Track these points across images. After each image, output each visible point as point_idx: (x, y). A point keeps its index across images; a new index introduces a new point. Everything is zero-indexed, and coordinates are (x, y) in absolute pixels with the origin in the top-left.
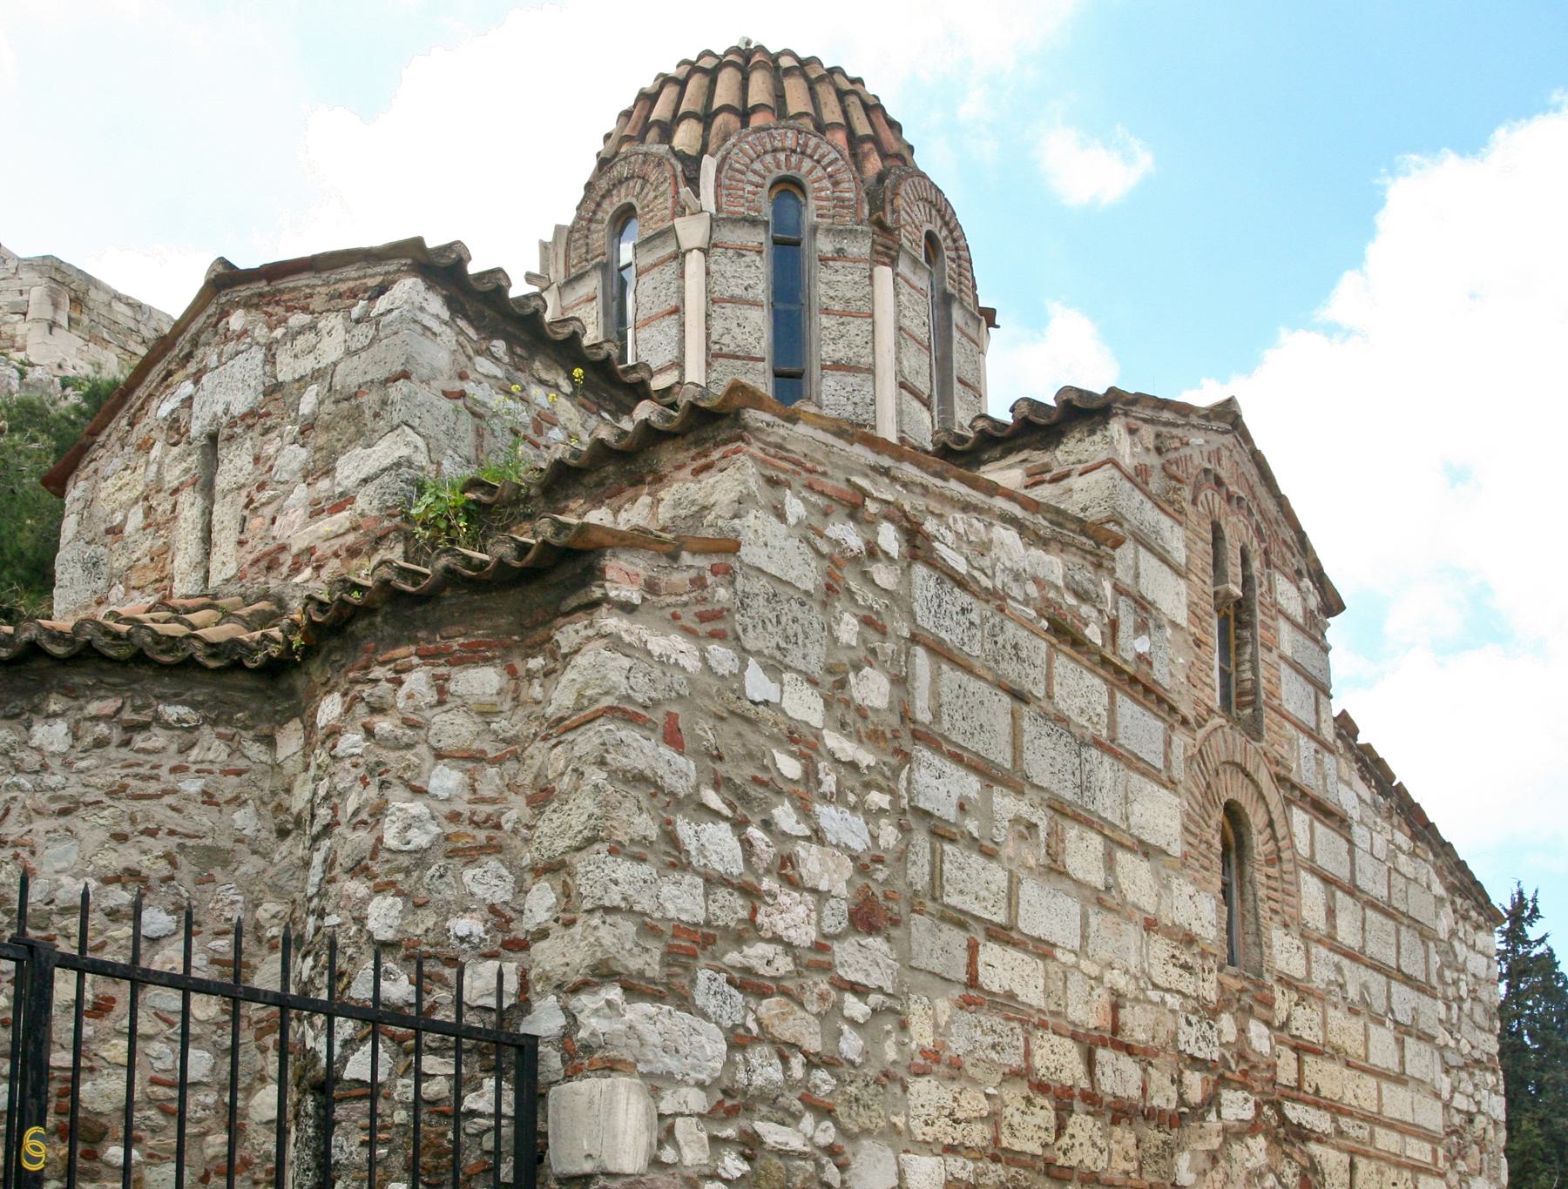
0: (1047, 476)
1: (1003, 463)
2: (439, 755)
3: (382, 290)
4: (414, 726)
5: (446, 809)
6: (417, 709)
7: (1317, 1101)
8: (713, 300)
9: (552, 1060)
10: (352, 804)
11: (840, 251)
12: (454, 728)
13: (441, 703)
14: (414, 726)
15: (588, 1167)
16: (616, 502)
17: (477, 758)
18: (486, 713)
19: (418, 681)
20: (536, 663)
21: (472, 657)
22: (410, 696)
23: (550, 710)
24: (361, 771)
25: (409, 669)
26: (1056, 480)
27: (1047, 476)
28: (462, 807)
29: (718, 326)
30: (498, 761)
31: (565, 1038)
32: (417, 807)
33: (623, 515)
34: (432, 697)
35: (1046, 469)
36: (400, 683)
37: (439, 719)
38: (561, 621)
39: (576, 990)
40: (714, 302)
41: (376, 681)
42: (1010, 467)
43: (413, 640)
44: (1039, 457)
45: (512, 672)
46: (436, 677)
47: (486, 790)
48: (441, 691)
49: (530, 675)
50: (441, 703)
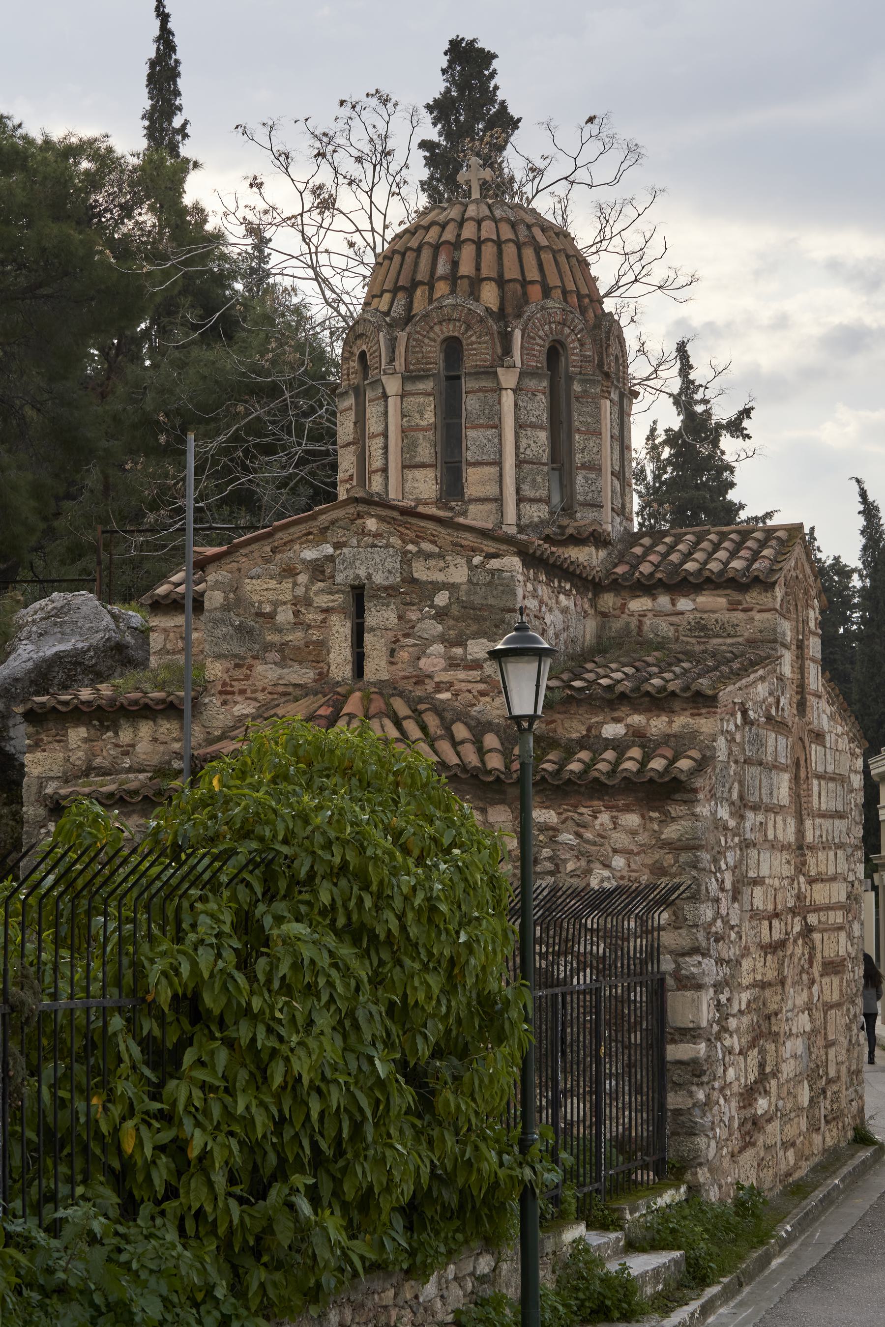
0: (740, 607)
1: (715, 592)
2: (615, 851)
3: (495, 556)
4: (603, 837)
5: (619, 874)
6: (605, 830)
7: (817, 909)
8: (520, 426)
9: (670, 982)
10: (570, 866)
11: (586, 391)
12: (620, 839)
13: (615, 828)
14: (603, 837)
15: (691, 1025)
16: (649, 715)
17: (630, 852)
18: (633, 833)
19: (604, 818)
20: (655, 815)
21: (627, 809)
22: (602, 825)
23: (663, 837)
24: (575, 853)
25: (600, 812)
26: (745, 610)
27: (740, 607)
28: (625, 873)
29: (524, 443)
30: (638, 854)
31: (676, 975)
32: (606, 873)
33: (653, 723)
34: (611, 826)
35: (739, 603)
36: (596, 818)
37: (615, 835)
38: (670, 802)
39: (683, 955)
40: (520, 426)
41: (582, 814)
42: (719, 596)
43: (599, 799)
44: (736, 596)
45: (643, 816)
46: (612, 817)
47: (633, 866)
48: (614, 823)
49: (651, 819)
50: (615, 828)
